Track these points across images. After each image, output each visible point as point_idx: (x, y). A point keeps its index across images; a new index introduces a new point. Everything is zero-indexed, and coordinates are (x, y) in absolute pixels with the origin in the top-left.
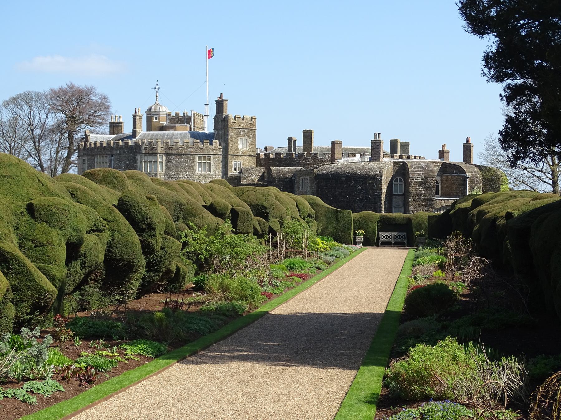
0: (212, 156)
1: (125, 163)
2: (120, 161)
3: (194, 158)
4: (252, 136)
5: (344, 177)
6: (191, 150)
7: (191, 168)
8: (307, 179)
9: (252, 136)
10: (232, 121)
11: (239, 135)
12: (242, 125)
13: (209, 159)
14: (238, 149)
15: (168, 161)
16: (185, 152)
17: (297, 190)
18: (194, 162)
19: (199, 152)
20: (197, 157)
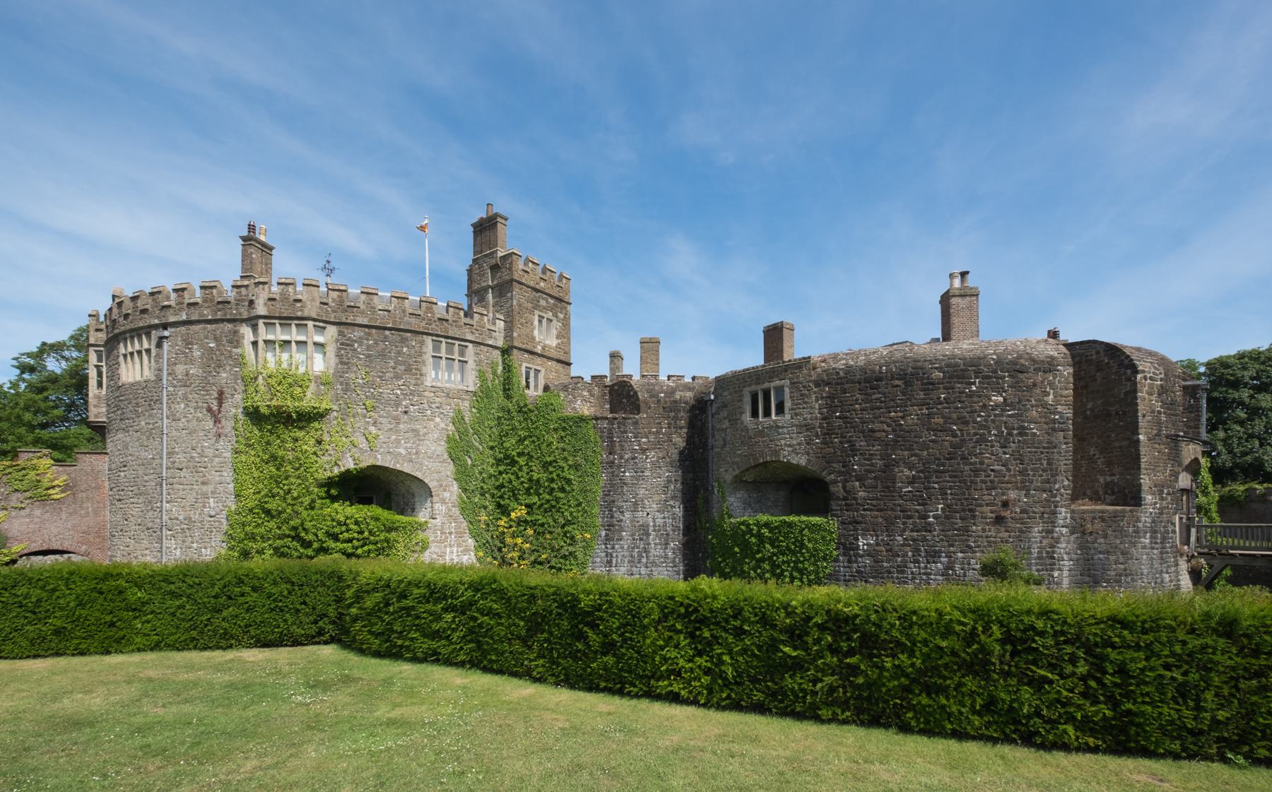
0: (470, 345)
1: (202, 346)
2: (188, 343)
3: (422, 343)
4: (561, 316)
5: (940, 369)
6: (413, 320)
7: (413, 369)
8: (780, 390)
9: (561, 316)
10: (521, 266)
11: (536, 307)
12: (542, 284)
13: (462, 353)
14: (534, 338)
15: (344, 345)
16: (394, 322)
17: (726, 424)
18: (420, 354)
19: (435, 328)
20: (429, 341)
